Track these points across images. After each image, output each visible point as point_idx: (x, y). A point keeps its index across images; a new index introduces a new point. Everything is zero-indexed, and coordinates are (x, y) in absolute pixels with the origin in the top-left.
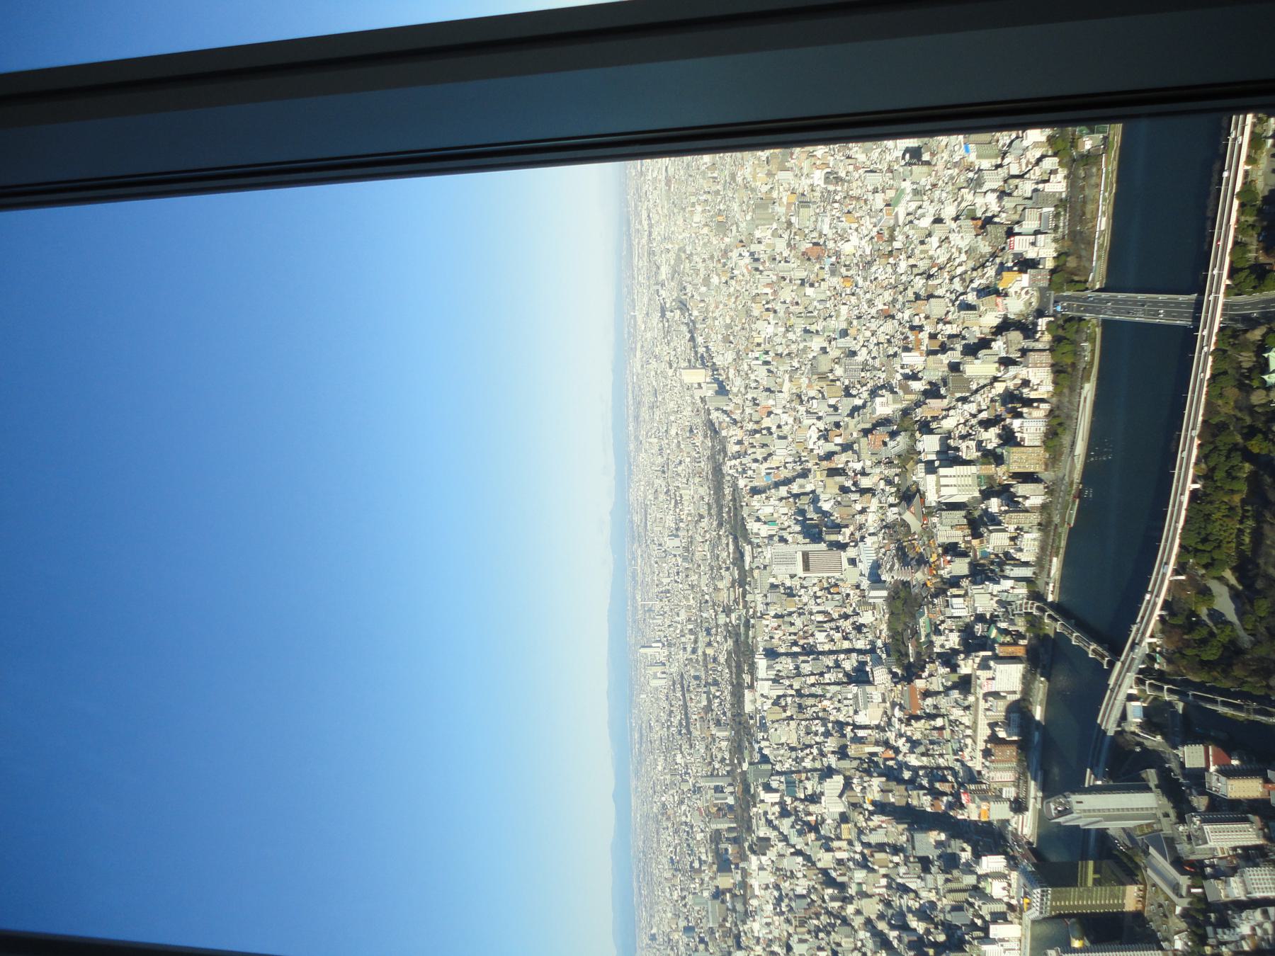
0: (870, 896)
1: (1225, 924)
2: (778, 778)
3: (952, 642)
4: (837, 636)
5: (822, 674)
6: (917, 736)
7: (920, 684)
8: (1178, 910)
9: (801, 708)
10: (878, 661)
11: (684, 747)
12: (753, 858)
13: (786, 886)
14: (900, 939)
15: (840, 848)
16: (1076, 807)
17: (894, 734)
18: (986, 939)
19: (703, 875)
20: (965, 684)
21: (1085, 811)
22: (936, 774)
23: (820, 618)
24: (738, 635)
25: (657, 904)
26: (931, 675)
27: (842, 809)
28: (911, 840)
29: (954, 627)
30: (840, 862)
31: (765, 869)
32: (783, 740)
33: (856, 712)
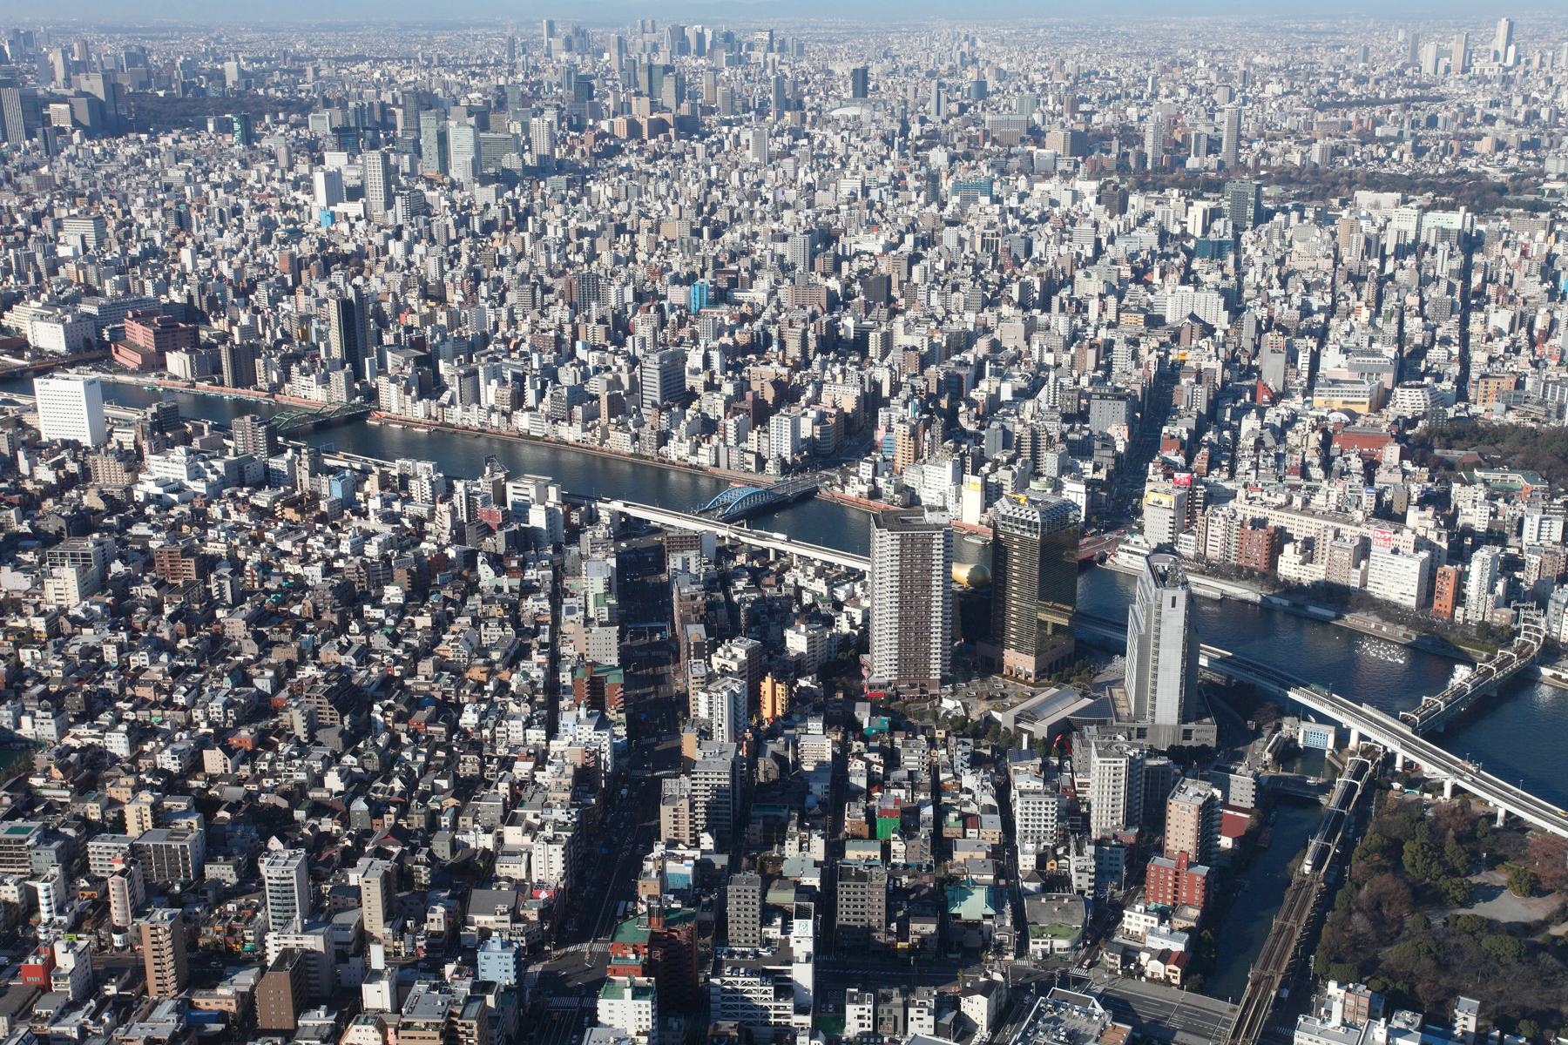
0: (1028, 339)
1: (976, 762)
2: (1230, 230)
3: (1471, 511)
4: (1500, 346)
5: (1421, 313)
6: (1292, 438)
7: (1392, 453)
8: (998, 716)
9: (1356, 279)
10: (1439, 400)
11: (1295, 98)
12: (1094, 185)
13: (1047, 229)
14: (964, 364)
15: (1104, 310)
16: (1168, 594)
17: (1298, 407)
18: (959, 471)
19: (1068, 115)
20: (1386, 513)
21: (1160, 606)
22: (1225, 455)
23: (1540, 323)
24: (1518, 191)
25: (1022, 51)
26: (1405, 473)
27: (1168, 320)
28: (1118, 395)
29: (1500, 518)
30: (1082, 307)
31: (1074, 202)
32: (1297, 246)
33: (1345, 351)
